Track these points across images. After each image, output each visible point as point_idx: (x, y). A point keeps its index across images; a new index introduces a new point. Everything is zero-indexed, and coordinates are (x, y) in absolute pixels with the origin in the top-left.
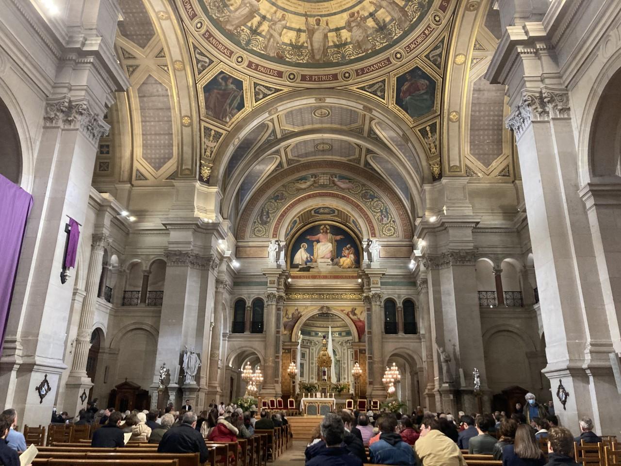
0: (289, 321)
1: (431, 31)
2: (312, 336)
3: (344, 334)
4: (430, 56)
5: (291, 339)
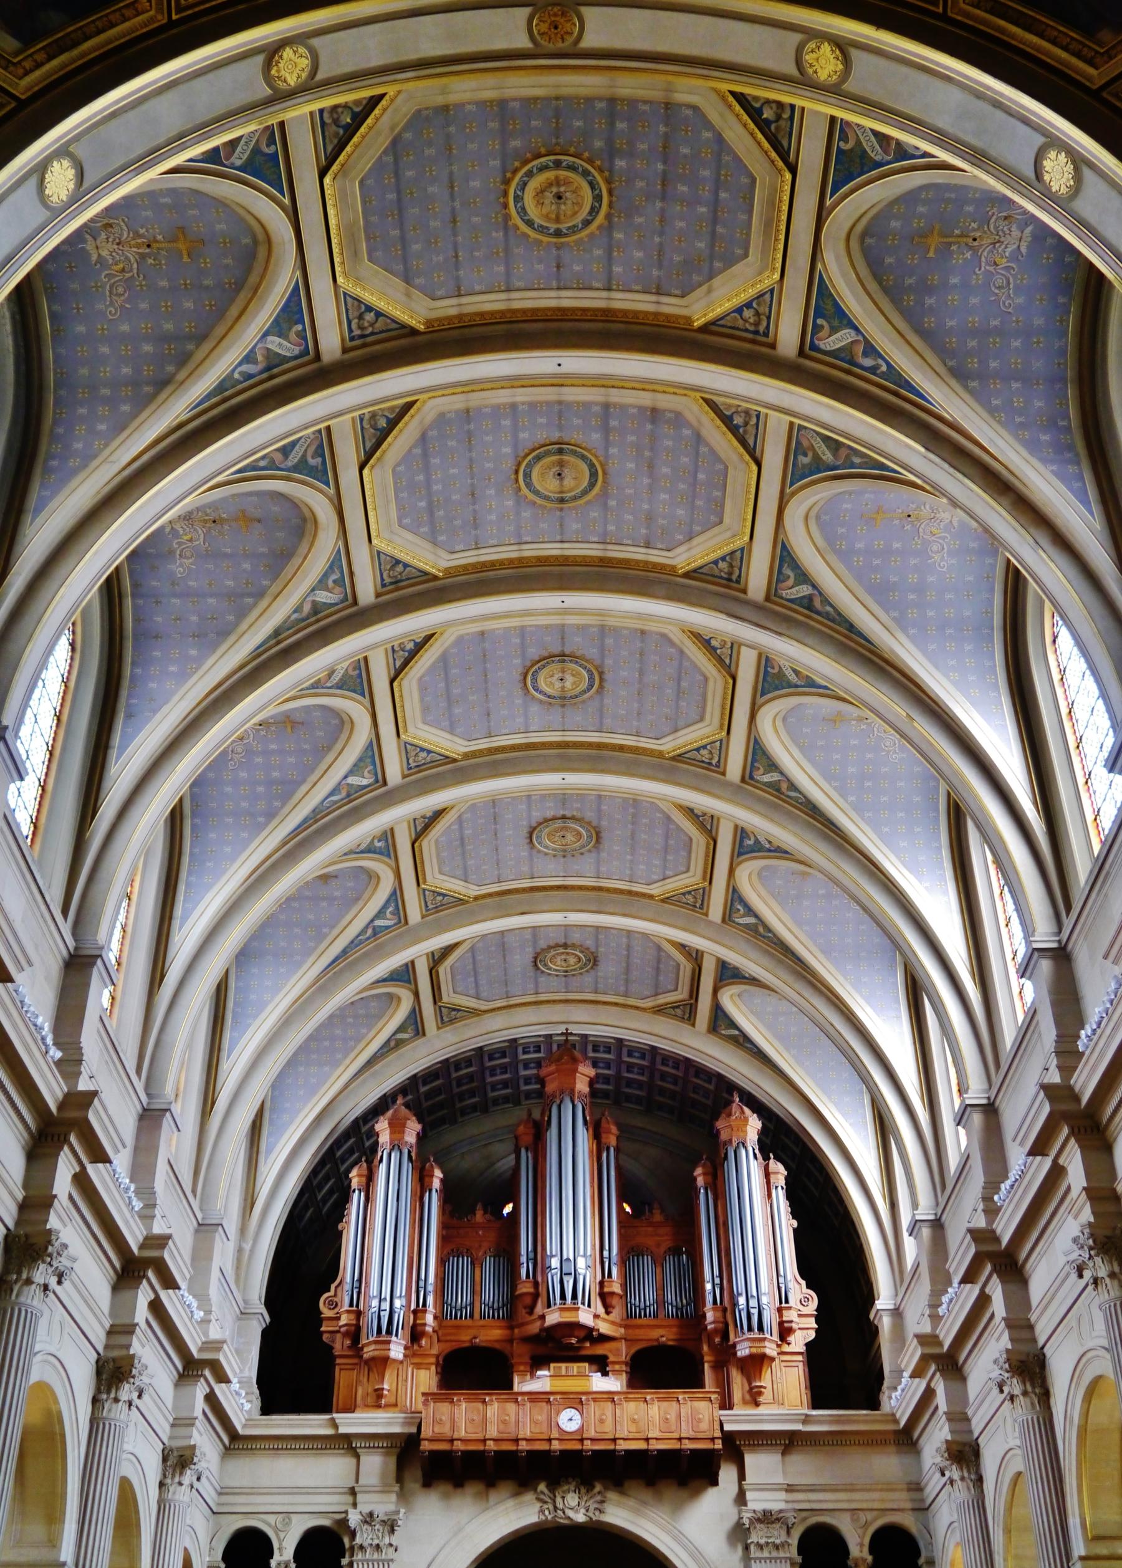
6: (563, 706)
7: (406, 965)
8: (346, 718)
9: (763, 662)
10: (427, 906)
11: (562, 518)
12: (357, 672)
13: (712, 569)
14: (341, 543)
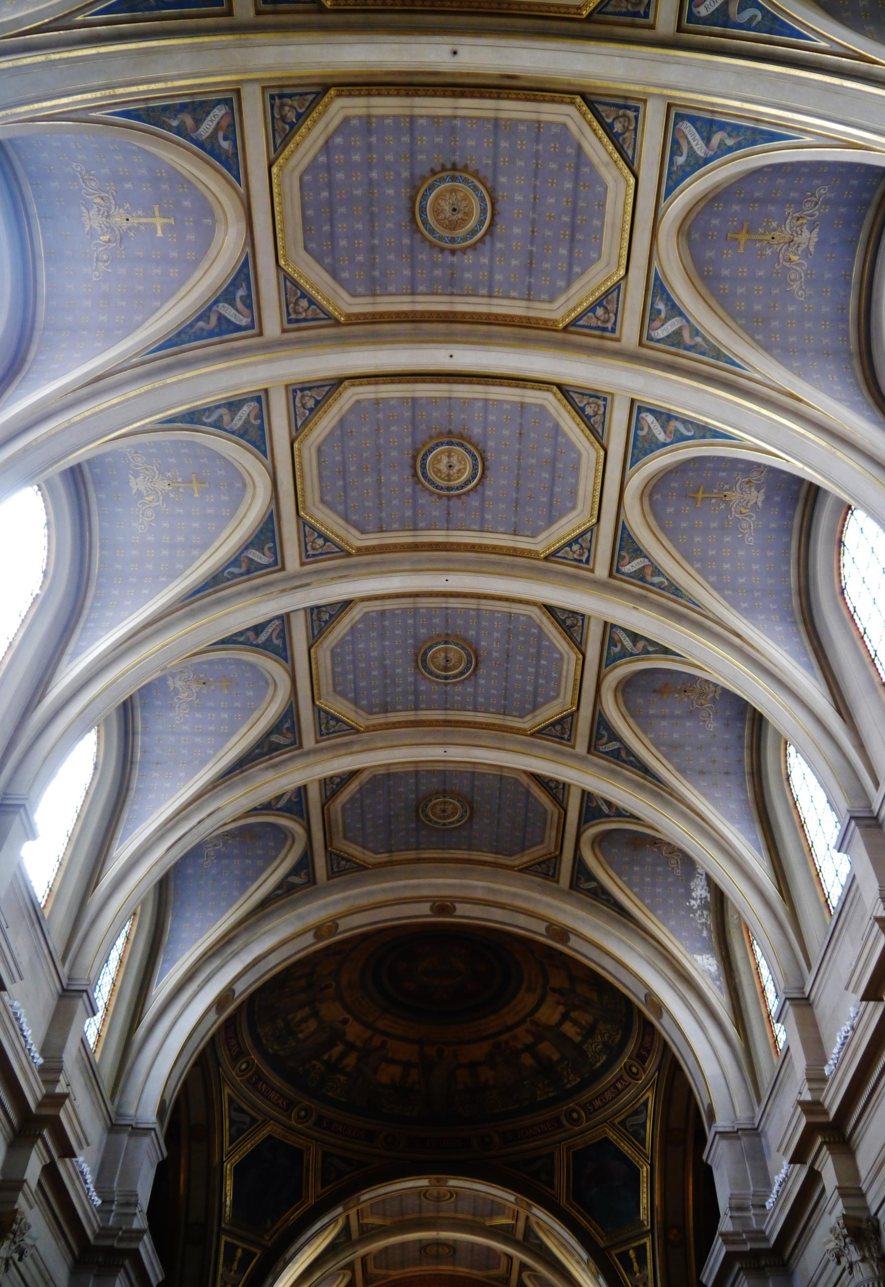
1: (626, 1087)
4: (628, 1125)
6: (450, 432)
7: (299, 788)
8: (270, 681)
9: (586, 798)
10: (332, 869)
11: (446, 627)
12: (259, 421)
13: (567, 552)
14: (248, 249)
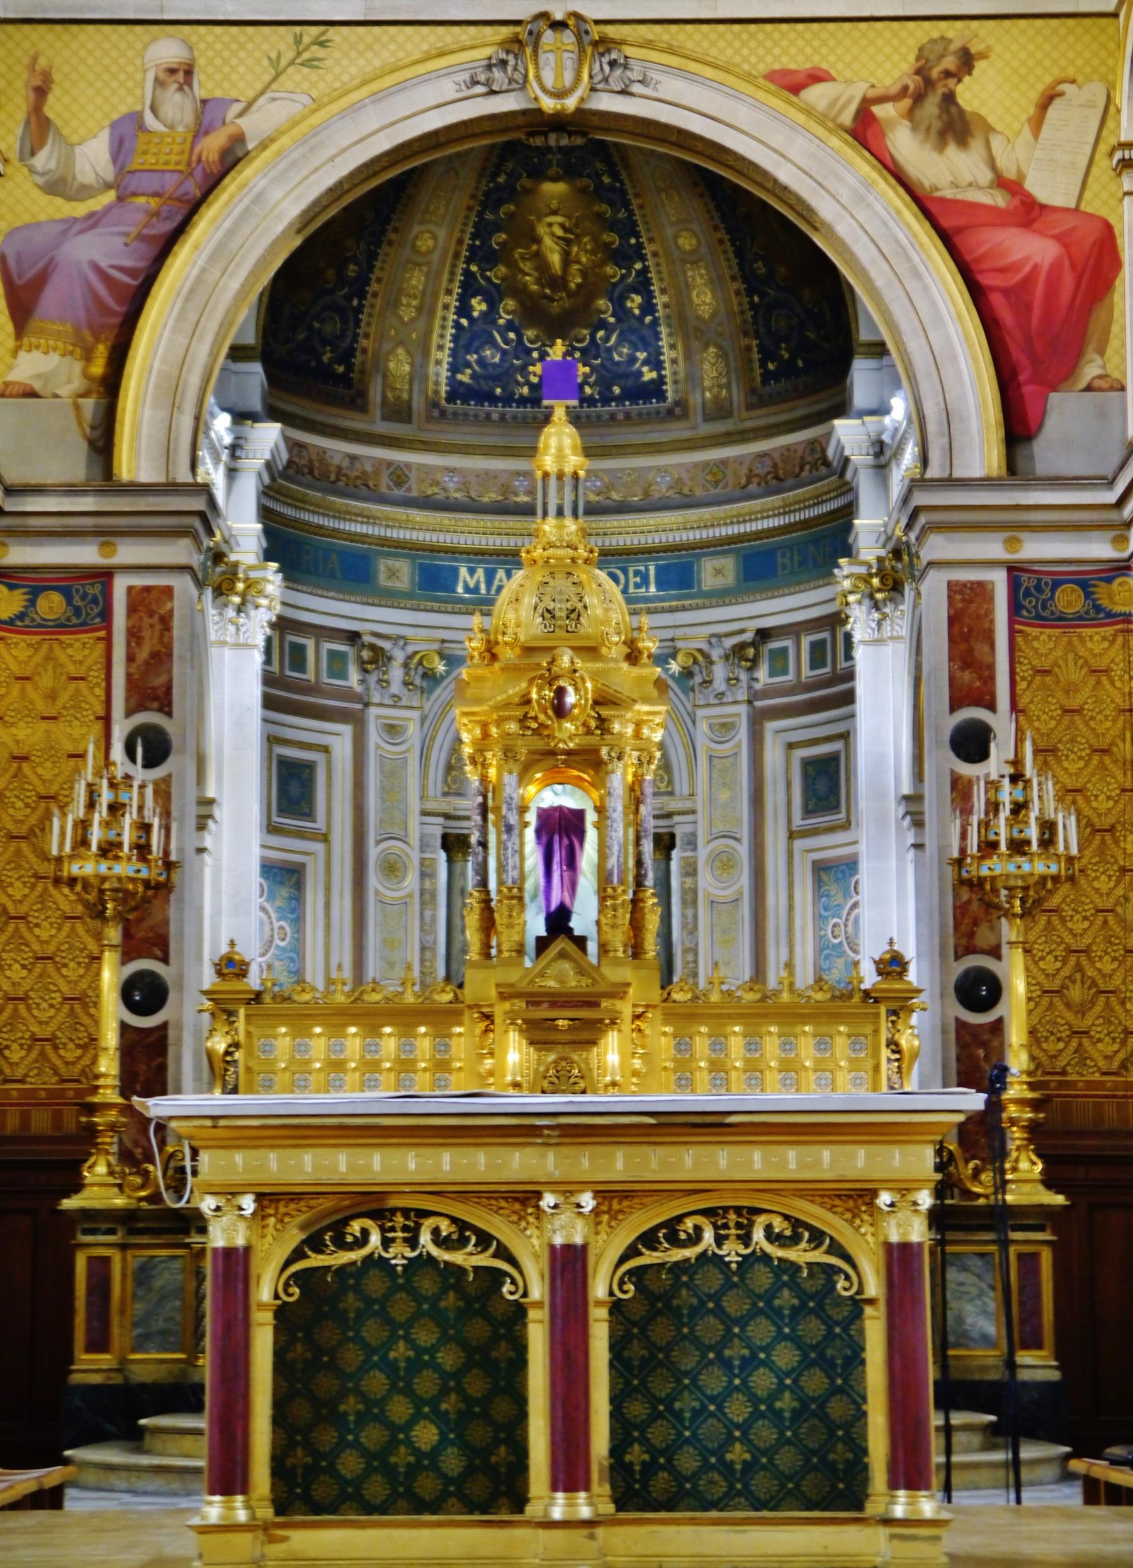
0: (69, 227)
2: (390, 598)
3: (716, 572)
5: (102, 443)
